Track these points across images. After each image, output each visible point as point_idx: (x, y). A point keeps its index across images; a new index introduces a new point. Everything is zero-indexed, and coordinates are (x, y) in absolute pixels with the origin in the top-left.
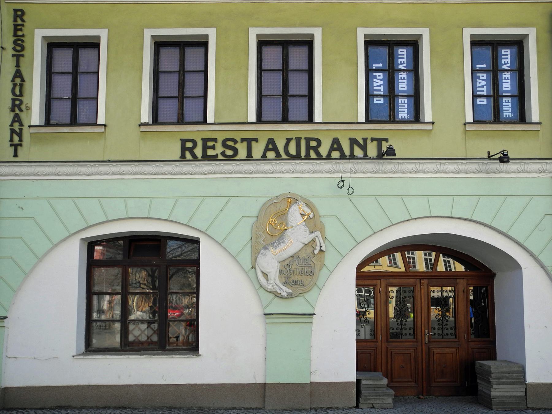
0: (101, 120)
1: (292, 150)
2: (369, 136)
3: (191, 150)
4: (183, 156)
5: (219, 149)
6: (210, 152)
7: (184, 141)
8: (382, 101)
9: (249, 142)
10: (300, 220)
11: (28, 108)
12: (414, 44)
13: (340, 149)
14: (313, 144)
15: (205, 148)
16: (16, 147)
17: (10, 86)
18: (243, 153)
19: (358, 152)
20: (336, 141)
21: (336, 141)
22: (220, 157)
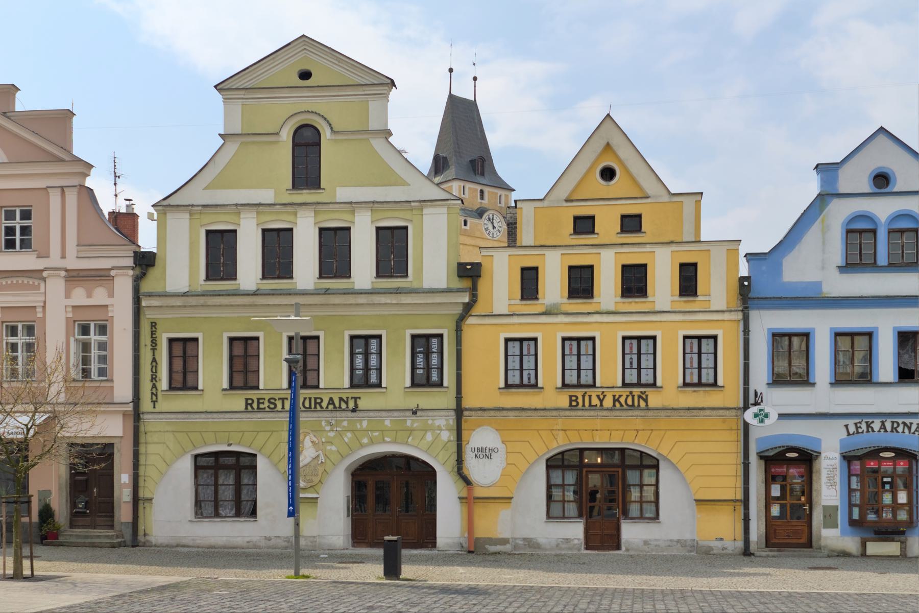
0: (200, 387)
1: (307, 405)
2: (350, 396)
3: (251, 405)
4: (246, 408)
5: (266, 404)
6: (261, 406)
7: (247, 400)
8: (361, 372)
9: (283, 400)
10: (311, 444)
11: (160, 380)
12: (379, 337)
13: (333, 404)
14: (319, 401)
15: (259, 403)
16: (154, 402)
17: (150, 367)
18: (279, 407)
19: (344, 406)
20: (331, 399)
21: (331, 399)
22: (267, 409)
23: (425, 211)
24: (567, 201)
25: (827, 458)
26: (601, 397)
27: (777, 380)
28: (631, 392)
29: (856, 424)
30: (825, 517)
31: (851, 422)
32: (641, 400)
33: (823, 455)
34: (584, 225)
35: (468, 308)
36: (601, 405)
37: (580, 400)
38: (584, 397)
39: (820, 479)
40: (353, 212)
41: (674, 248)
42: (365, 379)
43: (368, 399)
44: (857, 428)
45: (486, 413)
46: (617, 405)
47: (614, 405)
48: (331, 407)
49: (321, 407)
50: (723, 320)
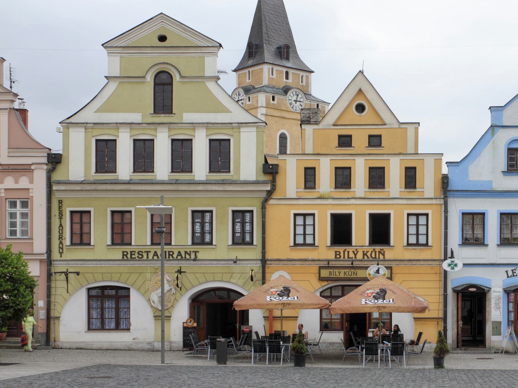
2: (192, 250)
20: (179, 252)
21: (179, 252)
23: (242, 130)
24: (334, 125)
25: (495, 292)
26: (356, 252)
27: (466, 242)
28: (374, 249)
29: (512, 270)
30: (493, 328)
31: (509, 269)
32: (380, 255)
33: (492, 290)
34: (345, 141)
35: (270, 193)
36: (355, 257)
37: (342, 254)
38: (344, 252)
39: (490, 304)
40: (194, 129)
41: (402, 157)
42: (201, 239)
43: (204, 253)
44: (513, 273)
45: (281, 263)
46: (366, 257)
47: (364, 258)
48: (179, 257)
49: (173, 257)
50: (432, 204)
